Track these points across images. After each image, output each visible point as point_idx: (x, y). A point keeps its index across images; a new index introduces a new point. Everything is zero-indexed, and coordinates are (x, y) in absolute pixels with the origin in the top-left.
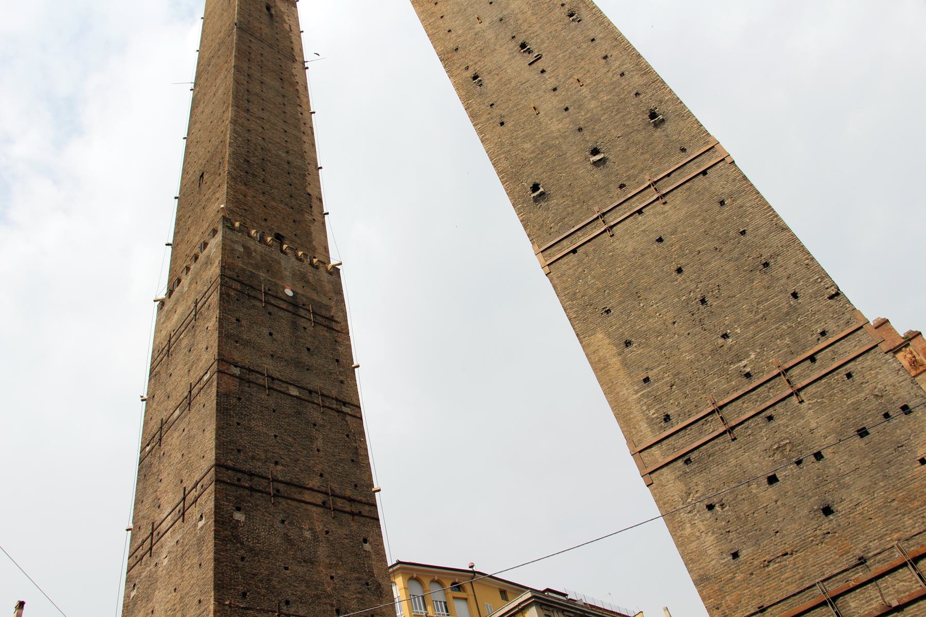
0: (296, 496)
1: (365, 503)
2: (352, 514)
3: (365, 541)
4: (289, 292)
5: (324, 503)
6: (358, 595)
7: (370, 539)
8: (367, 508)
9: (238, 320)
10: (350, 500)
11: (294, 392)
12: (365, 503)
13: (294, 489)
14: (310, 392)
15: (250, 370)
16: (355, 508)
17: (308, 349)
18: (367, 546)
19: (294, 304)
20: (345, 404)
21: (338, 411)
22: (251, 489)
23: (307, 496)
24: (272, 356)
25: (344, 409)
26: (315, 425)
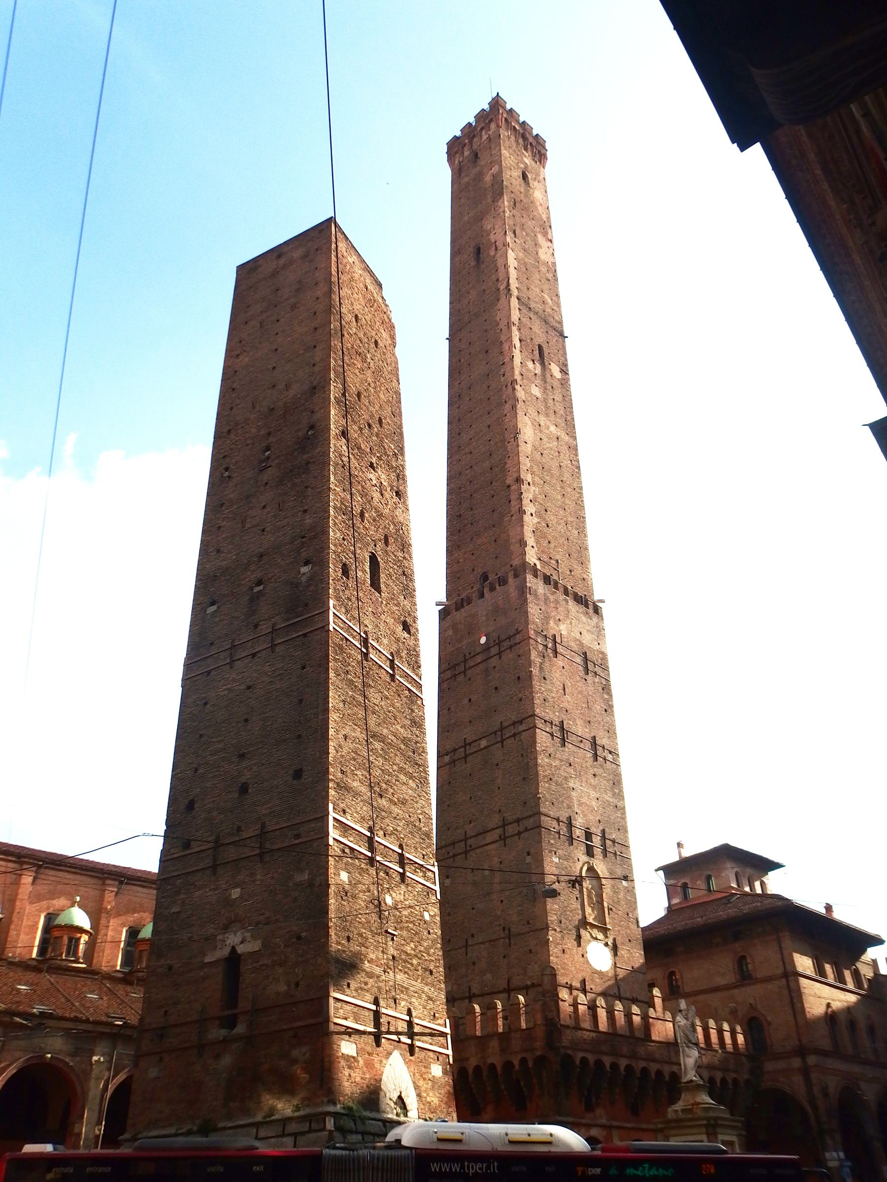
0: (482, 844)
1: (530, 816)
2: (519, 833)
3: (529, 854)
4: (483, 640)
5: (500, 837)
6: (519, 908)
7: (532, 851)
8: (532, 820)
9: (449, 709)
10: (518, 821)
11: (484, 743)
12: (530, 816)
13: (480, 837)
14: (495, 733)
15: (455, 750)
16: (521, 829)
17: (496, 688)
18: (528, 859)
19: (487, 648)
20: (521, 722)
21: (514, 735)
22: (455, 855)
23: (489, 838)
24: (470, 722)
25: (521, 728)
26: (497, 765)
